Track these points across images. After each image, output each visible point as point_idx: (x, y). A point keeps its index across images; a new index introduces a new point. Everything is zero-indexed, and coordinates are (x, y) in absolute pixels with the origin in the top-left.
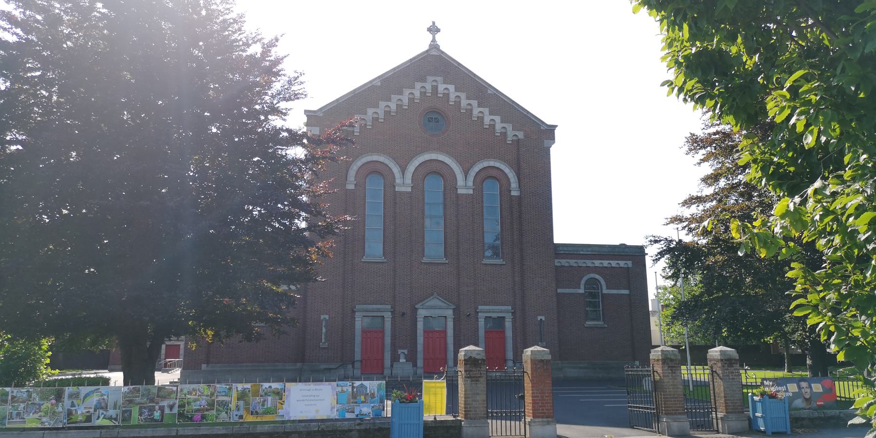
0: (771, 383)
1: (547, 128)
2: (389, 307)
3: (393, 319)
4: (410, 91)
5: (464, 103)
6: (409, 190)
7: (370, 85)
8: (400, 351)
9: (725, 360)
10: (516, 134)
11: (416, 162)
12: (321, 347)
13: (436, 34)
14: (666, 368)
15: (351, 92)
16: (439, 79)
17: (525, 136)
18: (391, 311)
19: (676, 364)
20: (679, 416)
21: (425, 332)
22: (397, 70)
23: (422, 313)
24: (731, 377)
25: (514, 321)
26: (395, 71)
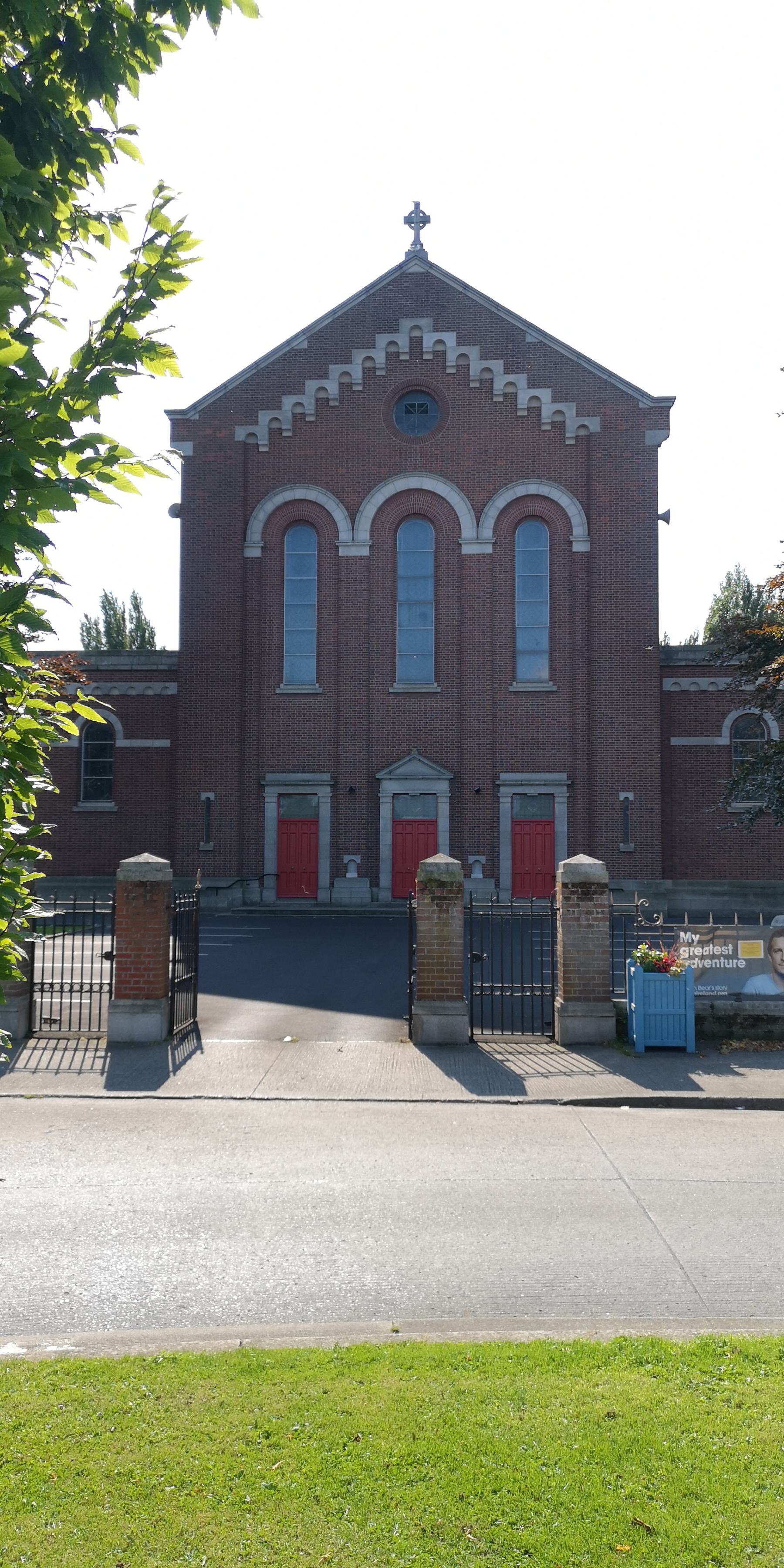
0: (696, 938)
1: (652, 405)
2: (326, 777)
3: (334, 797)
4: (364, 353)
5: (476, 367)
6: (365, 552)
7: (288, 349)
8: (346, 858)
9: (574, 885)
10: (586, 423)
11: (502, 500)
12: (200, 849)
13: (422, 227)
14: (426, 901)
15: (250, 368)
16: (425, 322)
17: (604, 427)
18: (331, 785)
19: (450, 891)
20: (448, 1004)
21: (515, 823)
22: (339, 314)
23: (389, 787)
24: (585, 923)
25: (571, 802)
26: (336, 316)
